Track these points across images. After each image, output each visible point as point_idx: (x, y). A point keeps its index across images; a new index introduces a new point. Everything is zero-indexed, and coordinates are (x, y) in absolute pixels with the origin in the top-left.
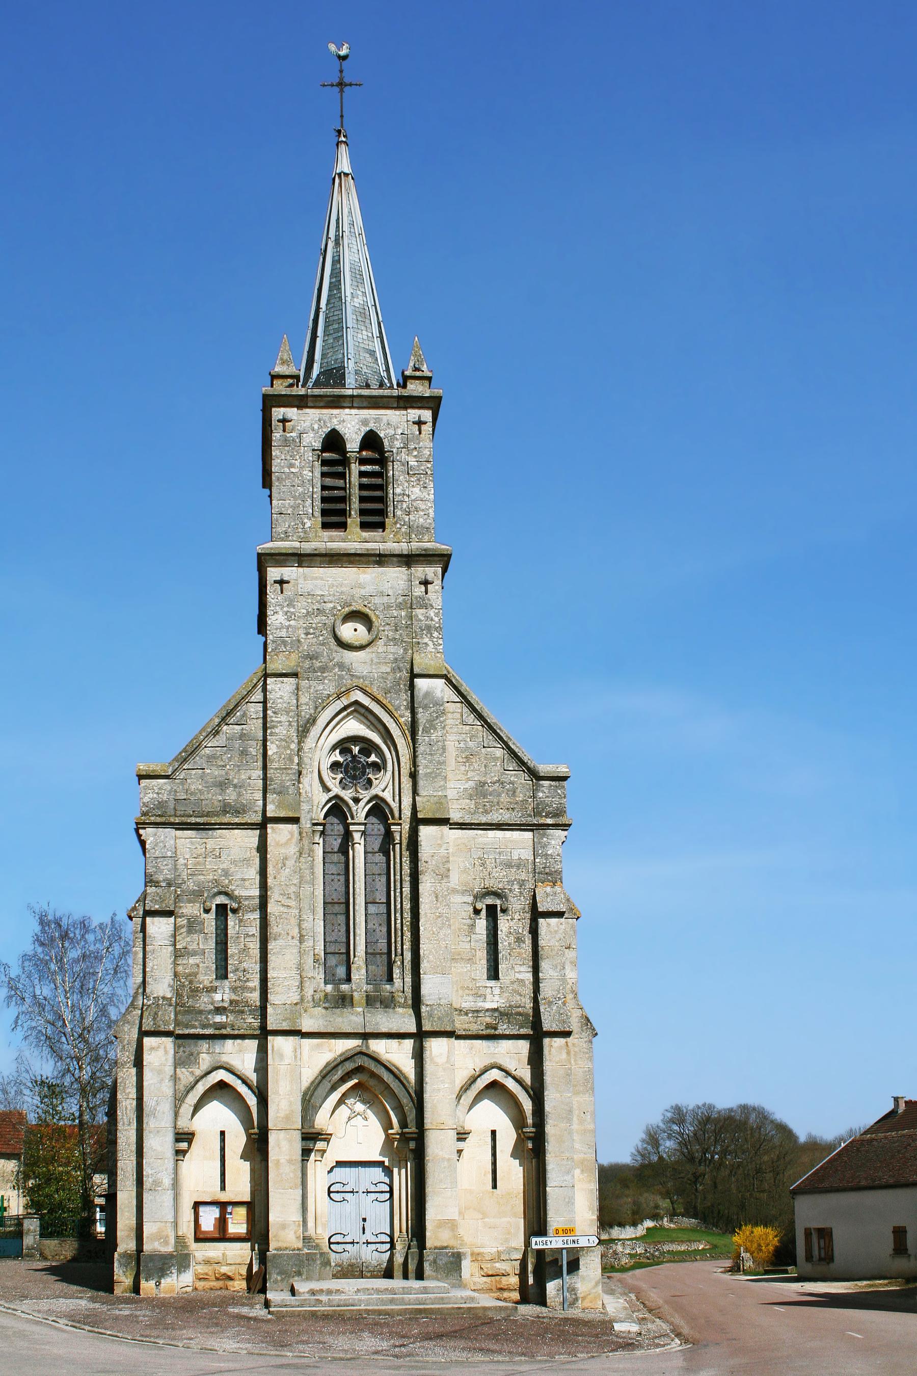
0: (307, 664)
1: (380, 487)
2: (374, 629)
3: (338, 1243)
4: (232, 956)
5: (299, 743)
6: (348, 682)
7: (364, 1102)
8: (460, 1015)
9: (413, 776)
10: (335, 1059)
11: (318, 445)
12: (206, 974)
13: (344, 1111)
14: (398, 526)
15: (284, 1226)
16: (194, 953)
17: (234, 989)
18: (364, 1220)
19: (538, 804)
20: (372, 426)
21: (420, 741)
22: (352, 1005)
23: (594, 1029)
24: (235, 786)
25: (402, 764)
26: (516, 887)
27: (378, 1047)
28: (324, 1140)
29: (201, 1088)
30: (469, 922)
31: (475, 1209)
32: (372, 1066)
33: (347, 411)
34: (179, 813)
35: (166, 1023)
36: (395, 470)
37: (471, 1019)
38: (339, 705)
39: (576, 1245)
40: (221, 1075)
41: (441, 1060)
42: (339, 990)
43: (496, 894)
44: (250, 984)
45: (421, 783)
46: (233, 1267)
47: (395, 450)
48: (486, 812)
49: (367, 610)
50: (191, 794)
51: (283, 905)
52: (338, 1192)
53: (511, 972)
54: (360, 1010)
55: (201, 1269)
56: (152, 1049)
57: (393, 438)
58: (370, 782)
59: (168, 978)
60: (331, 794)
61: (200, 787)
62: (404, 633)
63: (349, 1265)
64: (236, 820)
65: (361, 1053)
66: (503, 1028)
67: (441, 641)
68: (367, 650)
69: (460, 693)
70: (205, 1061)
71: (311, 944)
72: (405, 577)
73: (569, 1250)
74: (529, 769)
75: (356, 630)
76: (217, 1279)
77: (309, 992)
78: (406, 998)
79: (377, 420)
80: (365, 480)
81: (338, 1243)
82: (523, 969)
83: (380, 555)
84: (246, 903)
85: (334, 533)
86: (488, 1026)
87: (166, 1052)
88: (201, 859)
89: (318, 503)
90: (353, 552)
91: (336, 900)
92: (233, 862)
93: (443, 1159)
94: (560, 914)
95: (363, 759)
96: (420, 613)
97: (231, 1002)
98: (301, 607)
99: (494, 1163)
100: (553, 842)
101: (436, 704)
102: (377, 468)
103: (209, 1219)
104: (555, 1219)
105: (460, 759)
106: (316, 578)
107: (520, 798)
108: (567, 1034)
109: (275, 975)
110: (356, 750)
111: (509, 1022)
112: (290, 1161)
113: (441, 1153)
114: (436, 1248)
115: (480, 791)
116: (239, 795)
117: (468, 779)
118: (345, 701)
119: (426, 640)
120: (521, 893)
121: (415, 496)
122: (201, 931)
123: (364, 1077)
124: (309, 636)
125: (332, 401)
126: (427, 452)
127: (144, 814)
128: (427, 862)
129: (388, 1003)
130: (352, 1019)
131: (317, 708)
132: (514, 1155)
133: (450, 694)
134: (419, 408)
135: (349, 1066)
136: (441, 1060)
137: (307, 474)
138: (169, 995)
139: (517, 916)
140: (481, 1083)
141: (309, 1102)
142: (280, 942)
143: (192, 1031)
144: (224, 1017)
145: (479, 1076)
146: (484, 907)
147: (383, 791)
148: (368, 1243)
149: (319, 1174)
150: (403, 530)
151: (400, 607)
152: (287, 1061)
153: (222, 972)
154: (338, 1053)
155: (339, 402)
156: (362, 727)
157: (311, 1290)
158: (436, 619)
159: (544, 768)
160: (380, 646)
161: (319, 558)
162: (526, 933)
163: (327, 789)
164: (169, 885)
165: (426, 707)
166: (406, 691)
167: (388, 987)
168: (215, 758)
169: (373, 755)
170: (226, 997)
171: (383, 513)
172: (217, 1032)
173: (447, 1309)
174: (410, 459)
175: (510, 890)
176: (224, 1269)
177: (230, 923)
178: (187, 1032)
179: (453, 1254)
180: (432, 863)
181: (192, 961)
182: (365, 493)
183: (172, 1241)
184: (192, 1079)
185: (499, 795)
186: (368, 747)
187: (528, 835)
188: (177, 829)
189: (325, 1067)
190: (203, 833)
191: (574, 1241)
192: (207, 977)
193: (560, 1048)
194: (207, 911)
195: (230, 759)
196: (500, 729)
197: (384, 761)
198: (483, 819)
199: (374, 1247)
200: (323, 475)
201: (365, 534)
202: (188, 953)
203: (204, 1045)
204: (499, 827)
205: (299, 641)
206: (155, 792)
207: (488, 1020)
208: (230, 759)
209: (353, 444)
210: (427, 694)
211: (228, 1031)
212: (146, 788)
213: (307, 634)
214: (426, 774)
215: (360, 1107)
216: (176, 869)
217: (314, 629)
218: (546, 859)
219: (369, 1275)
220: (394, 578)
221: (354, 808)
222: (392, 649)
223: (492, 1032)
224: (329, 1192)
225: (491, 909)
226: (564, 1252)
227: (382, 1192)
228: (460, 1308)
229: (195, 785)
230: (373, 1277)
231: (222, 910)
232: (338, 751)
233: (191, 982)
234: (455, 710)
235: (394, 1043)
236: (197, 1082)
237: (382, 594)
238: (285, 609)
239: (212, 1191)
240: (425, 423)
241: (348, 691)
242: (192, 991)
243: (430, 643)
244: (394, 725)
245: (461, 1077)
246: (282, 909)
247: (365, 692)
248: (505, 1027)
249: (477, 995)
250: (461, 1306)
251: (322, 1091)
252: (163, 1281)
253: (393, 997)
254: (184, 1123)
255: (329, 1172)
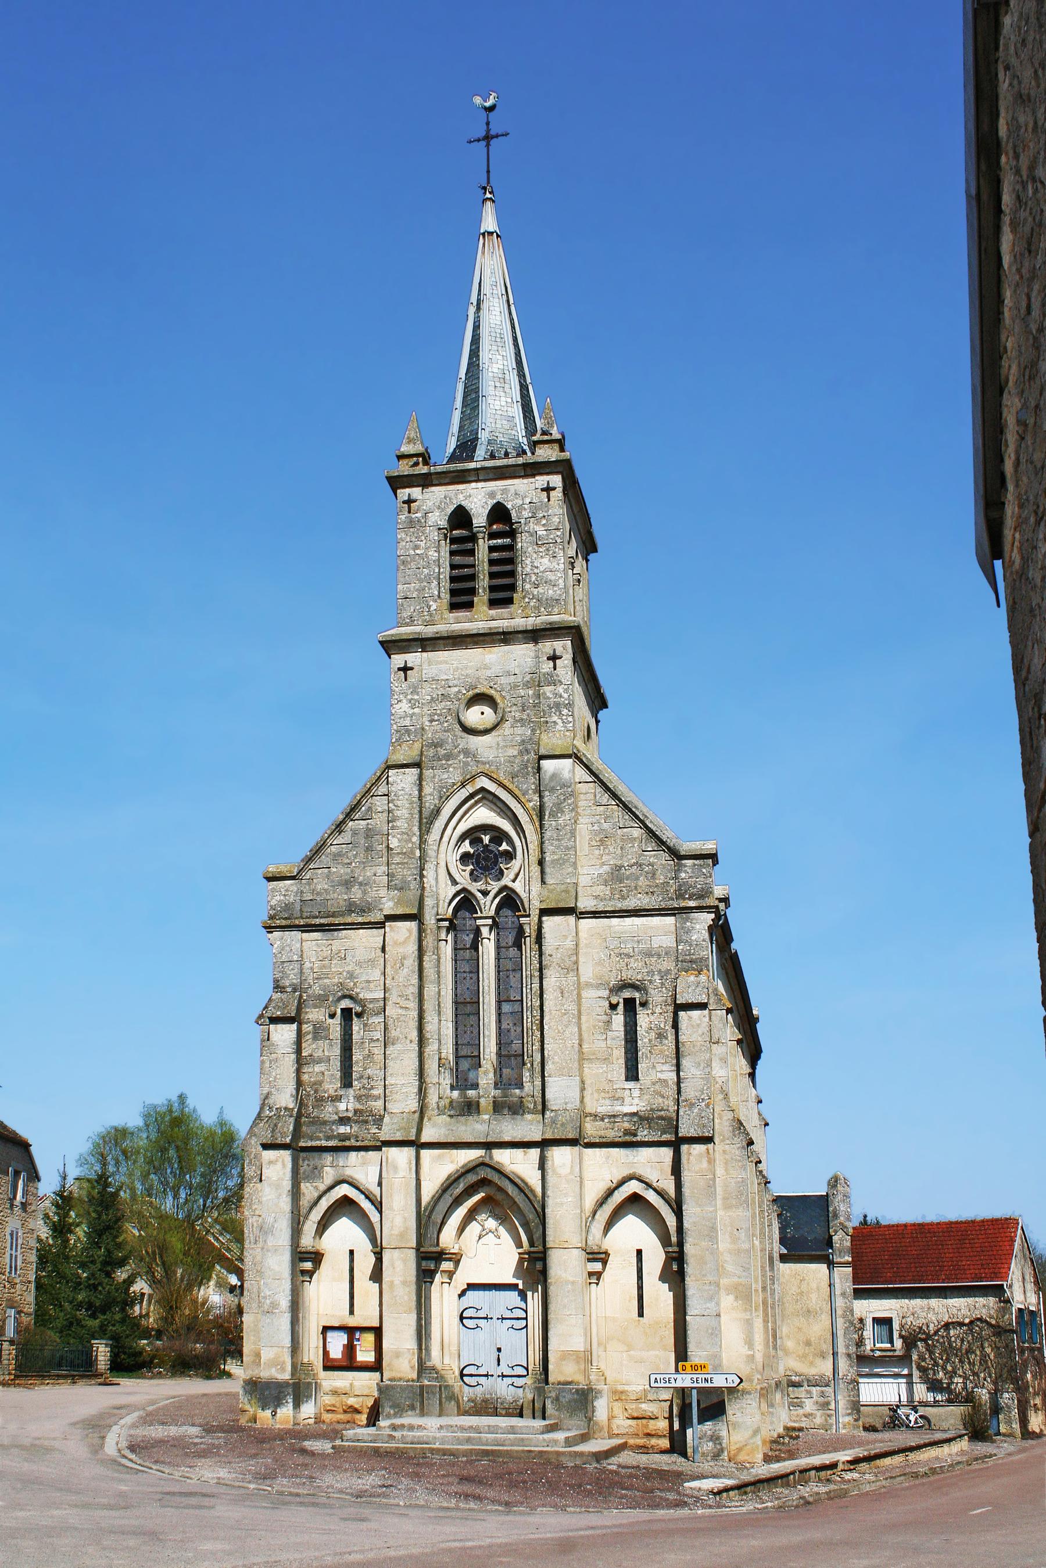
0: (431, 752)
1: (511, 561)
2: (500, 711)
3: (471, 1375)
4: (357, 1062)
5: (421, 837)
6: (474, 769)
7: (496, 1217)
8: (595, 1120)
9: (541, 863)
10: (458, 1171)
11: (443, 523)
12: (331, 1082)
13: (474, 1228)
14: (527, 600)
15: (397, 1355)
16: (319, 1061)
17: (358, 1098)
18: (499, 1350)
19: (680, 886)
20: (499, 498)
21: (547, 826)
22: (478, 1112)
23: (748, 1134)
24: (361, 884)
25: (531, 851)
26: (657, 977)
27: (503, 1157)
28: (450, 1260)
29: (324, 1204)
30: (605, 1018)
31: (618, 1340)
32: (495, 1178)
33: (473, 485)
34: (305, 914)
35: (284, 1135)
36: (523, 542)
37: (608, 1125)
38: (464, 793)
39: (709, 1385)
40: (344, 1190)
41: (565, 1171)
42: (465, 1097)
43: (634, 987)
44: (375, 1092)
45: (548, 870)
46: (361, 1399)
47: (522, 521)
48: (623, 898)
49: (492, 692)
50: (318, 894)
51: (401, 1007)
52: (471, 1318)
53: (653, 1072)
54: (486, 1117)
55: (328, 1400)
56: (270, 1162)
57: (521, 508)
58: (502, 873)
59: (291, 1087)
60: (459, 887)
61: (326, 887)
62: (532, 713)
63: (483, 1401)
64: (360, 920)
65: (483, 1164)
66: (644, 1134)
67: (570, 719)
68: (493, 733)
69: (592, 773)
70: (329, 1175)
71: (436, 1047)
72: (532, 654)
73: (700, 1390)
74: (669, 848)
75: (482, 713)
76: (345, 1412)
77: (432, 1099)
78: (535, 1102)
79: (505, 491)
80: (495, 555)
81: (471, 1375)
82: (665, 1067)
83: (504, 633)
84: (371, 1006)
85: (462, 614)
86: (627, 1132)
87: (284, 1165)
88: (327, 962)
89: (446, 585)
90: (475, 632)
91: (468, 1000)
92: (359, 964)
93: (567, 1282)
94: (702, 1006)
95: (493, 847)
96: (548, 690)
97: (356, 1111)
98: (426, 693)
99: (640, 1288)
100: (698, 927)
101: (563, 786)
102: (508, 541)
103: (337, 1344)
104: (696, 1354)
105: (594, 843)
106: (441, 663)
107: (660, 879)
108: (708, 1140)
109: (393, 1082)
110: (486, 839)
111: (650, 1128)
112: (404, 1283)
113: (564, 1275)
114: (559, 1383)
115: (616, 875)
116: (365, 893)
117: (603, 864)
118: (470, 789)
119: (555, 718)
120: (662, 984)
121: (546, 564)
122: (327, 1038)
123: (491, 1191)
124: (434, 723)
125: (457, 476)
126: (556, 520)
127: (271, 918)
128: (551, 956)
129: (516, 1109)
130: (475, 1128)
131: (441, 797)
132: (663, 1278)
133: (581, 773)
134: (548, 474)
135: (472, 1178)
136: (565, 1171)
137: (433, 554)
138: (291, 1106)
139: (658, 1010)
140: (619, 1196)
141: (428, 1221)
142: (399, 1046)
143: (317, 1143)
144: (348, 1128)
145: (616, 1188)
146: (621, 1001)
147: (514, 881)
148: (503, 1376)
149: (444, 1298)
150: (532, 604)
151: (527, 685)
152: (401, 1174)
153: (347, 1081)
154: (461, 1164)
155: (465, 476)
156: (493, 814)
157: (392, 1424)
158: (566, 696)
159: (687, 847)
160: (506, 728)
161: (441, 642)
162: (668, 1027)
163: (455, 882)
164: (295, 990)
165: (552, 790)
166: (534, 774)
167: (517, 1091)
168: (340, 856)
169: (504, 844)
170: (351, 1107)
171: (512, 588)
172: (340, 1144)
173: (517, 1451)
174: (537, 528)
175: (650, 981)
176: (351, 1401)
177: (355, 1028)
178: (310, 1144)
179: (577, 1390)
180: (557, 956)
181: (318, 1068)
182: (496, 569)
183: (289, 1368)
184: (316, 1195)
185: (637, 879)
186: (499, 836)
187: (670, 920)
188: (303, 932)
189: (447, 1179)
190: (329, 935)
191: (706, 1380)
192: (332, 1086)
193: (700, 1155)
194: (332, 1016)
195: (355, 856)
196: (636, 807)
197: (514, 849)
198: (620, 905)
199: (509, 1380)
200: (452, 553)
201: (493, 612)
202: (314, 1061)
203: (328, 1158)
204: (636, 913)
205: (423, 729)
206: (285, 892)
207: (626, 1125)
208: (355, 856)
209: (480, 520)
210: (554, 776)
211: (353, 1142)
212: (273, 890)
213: (431, 721)
214: (553, 861)
215: (491, 1223)
216: (301, 972)
217: (439, 715)
218: (690, 946)
219: (504, 1412)
220: (521, 656)
221: (482, 902)
222: (519, 730)
223: (628, 1138)
224: (462, 1318)
225: (630, 1004)
226: (694, 1392)
227: (518, 1319)
228: (530, 1451)
229: (321, 885)
230: (508, 1415)
231: (347, 1013)
232: (467, 842)
233: (316, 1091)
234: (588, 790)
235: (518, 1153)
236: (320, 1197)
237: (508, 674)
238: (409, 697)
239: (339, 1315)
240: (554, 489)
241: (473, 778)
242: (317, 1101)
243: (559, 721)
244: (522, 810)
245: (593, 1193)
246: (400, 1011)
247: (491, 778)
248: (645, 1133)
249: (614, 1098)
250: (532, 1449)
251: (442, 1207)
252: (278, 1410)
253: (522, 1102)
254: (307, 1241)
255: (460, 1296)
